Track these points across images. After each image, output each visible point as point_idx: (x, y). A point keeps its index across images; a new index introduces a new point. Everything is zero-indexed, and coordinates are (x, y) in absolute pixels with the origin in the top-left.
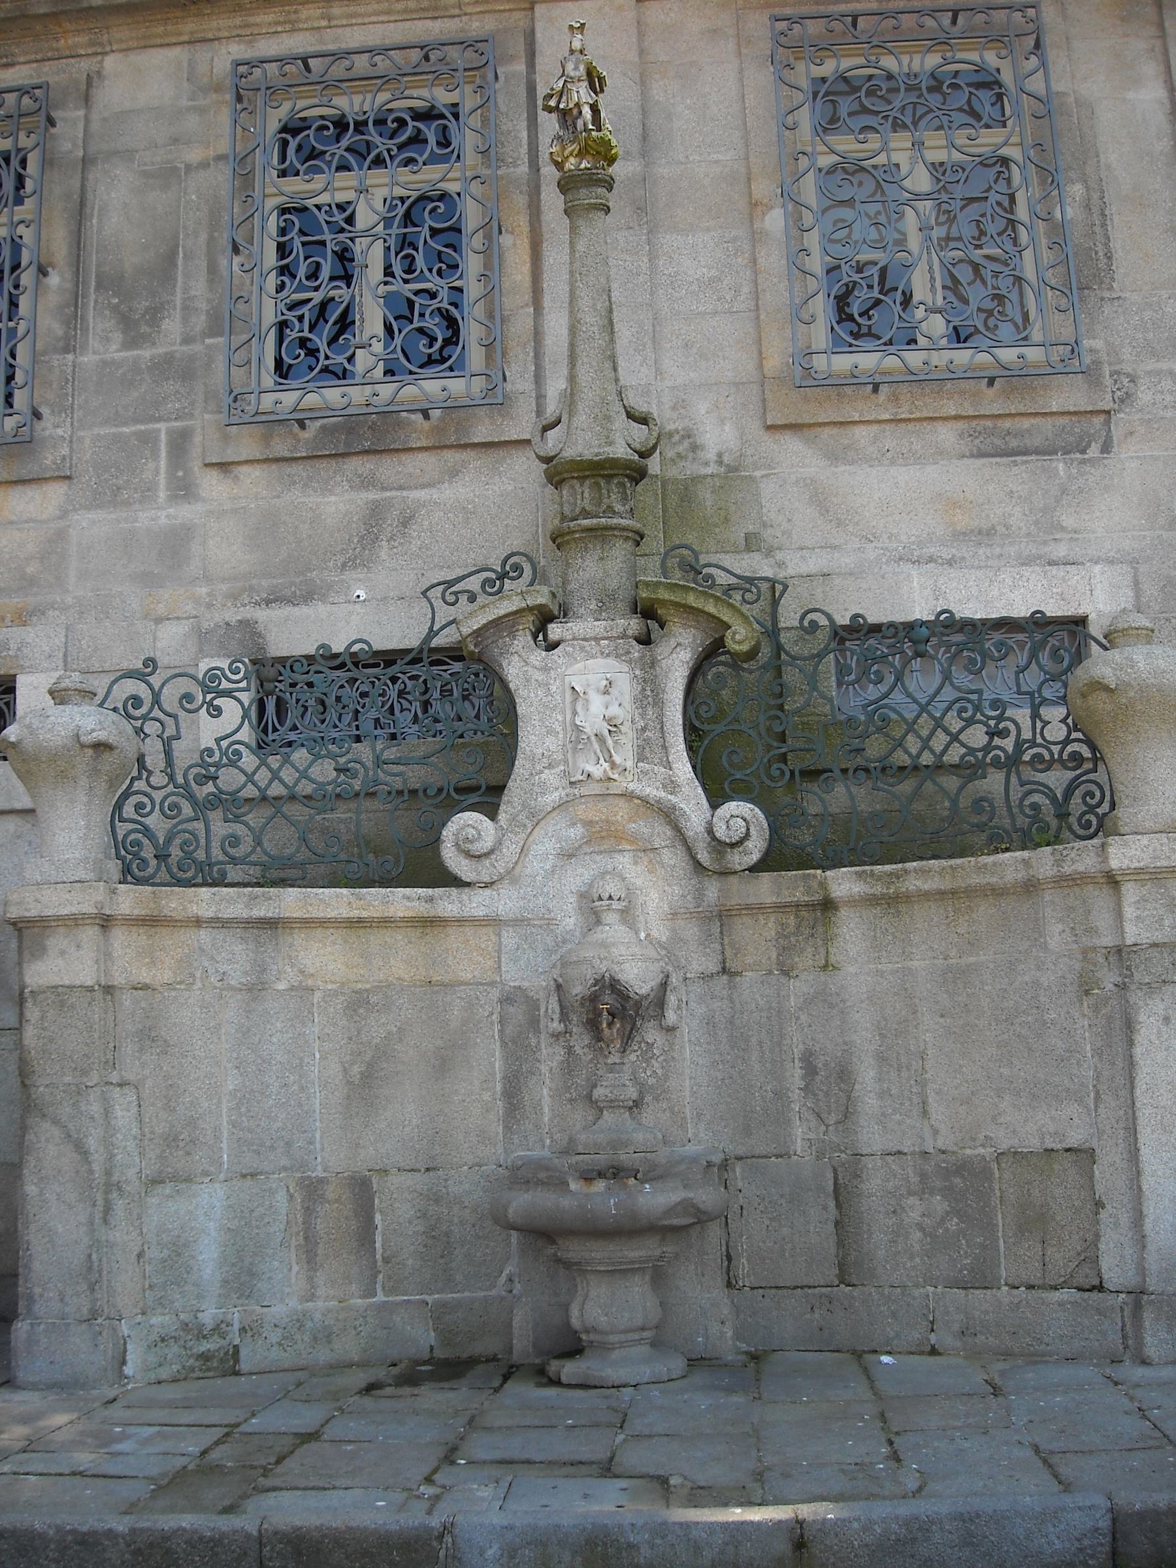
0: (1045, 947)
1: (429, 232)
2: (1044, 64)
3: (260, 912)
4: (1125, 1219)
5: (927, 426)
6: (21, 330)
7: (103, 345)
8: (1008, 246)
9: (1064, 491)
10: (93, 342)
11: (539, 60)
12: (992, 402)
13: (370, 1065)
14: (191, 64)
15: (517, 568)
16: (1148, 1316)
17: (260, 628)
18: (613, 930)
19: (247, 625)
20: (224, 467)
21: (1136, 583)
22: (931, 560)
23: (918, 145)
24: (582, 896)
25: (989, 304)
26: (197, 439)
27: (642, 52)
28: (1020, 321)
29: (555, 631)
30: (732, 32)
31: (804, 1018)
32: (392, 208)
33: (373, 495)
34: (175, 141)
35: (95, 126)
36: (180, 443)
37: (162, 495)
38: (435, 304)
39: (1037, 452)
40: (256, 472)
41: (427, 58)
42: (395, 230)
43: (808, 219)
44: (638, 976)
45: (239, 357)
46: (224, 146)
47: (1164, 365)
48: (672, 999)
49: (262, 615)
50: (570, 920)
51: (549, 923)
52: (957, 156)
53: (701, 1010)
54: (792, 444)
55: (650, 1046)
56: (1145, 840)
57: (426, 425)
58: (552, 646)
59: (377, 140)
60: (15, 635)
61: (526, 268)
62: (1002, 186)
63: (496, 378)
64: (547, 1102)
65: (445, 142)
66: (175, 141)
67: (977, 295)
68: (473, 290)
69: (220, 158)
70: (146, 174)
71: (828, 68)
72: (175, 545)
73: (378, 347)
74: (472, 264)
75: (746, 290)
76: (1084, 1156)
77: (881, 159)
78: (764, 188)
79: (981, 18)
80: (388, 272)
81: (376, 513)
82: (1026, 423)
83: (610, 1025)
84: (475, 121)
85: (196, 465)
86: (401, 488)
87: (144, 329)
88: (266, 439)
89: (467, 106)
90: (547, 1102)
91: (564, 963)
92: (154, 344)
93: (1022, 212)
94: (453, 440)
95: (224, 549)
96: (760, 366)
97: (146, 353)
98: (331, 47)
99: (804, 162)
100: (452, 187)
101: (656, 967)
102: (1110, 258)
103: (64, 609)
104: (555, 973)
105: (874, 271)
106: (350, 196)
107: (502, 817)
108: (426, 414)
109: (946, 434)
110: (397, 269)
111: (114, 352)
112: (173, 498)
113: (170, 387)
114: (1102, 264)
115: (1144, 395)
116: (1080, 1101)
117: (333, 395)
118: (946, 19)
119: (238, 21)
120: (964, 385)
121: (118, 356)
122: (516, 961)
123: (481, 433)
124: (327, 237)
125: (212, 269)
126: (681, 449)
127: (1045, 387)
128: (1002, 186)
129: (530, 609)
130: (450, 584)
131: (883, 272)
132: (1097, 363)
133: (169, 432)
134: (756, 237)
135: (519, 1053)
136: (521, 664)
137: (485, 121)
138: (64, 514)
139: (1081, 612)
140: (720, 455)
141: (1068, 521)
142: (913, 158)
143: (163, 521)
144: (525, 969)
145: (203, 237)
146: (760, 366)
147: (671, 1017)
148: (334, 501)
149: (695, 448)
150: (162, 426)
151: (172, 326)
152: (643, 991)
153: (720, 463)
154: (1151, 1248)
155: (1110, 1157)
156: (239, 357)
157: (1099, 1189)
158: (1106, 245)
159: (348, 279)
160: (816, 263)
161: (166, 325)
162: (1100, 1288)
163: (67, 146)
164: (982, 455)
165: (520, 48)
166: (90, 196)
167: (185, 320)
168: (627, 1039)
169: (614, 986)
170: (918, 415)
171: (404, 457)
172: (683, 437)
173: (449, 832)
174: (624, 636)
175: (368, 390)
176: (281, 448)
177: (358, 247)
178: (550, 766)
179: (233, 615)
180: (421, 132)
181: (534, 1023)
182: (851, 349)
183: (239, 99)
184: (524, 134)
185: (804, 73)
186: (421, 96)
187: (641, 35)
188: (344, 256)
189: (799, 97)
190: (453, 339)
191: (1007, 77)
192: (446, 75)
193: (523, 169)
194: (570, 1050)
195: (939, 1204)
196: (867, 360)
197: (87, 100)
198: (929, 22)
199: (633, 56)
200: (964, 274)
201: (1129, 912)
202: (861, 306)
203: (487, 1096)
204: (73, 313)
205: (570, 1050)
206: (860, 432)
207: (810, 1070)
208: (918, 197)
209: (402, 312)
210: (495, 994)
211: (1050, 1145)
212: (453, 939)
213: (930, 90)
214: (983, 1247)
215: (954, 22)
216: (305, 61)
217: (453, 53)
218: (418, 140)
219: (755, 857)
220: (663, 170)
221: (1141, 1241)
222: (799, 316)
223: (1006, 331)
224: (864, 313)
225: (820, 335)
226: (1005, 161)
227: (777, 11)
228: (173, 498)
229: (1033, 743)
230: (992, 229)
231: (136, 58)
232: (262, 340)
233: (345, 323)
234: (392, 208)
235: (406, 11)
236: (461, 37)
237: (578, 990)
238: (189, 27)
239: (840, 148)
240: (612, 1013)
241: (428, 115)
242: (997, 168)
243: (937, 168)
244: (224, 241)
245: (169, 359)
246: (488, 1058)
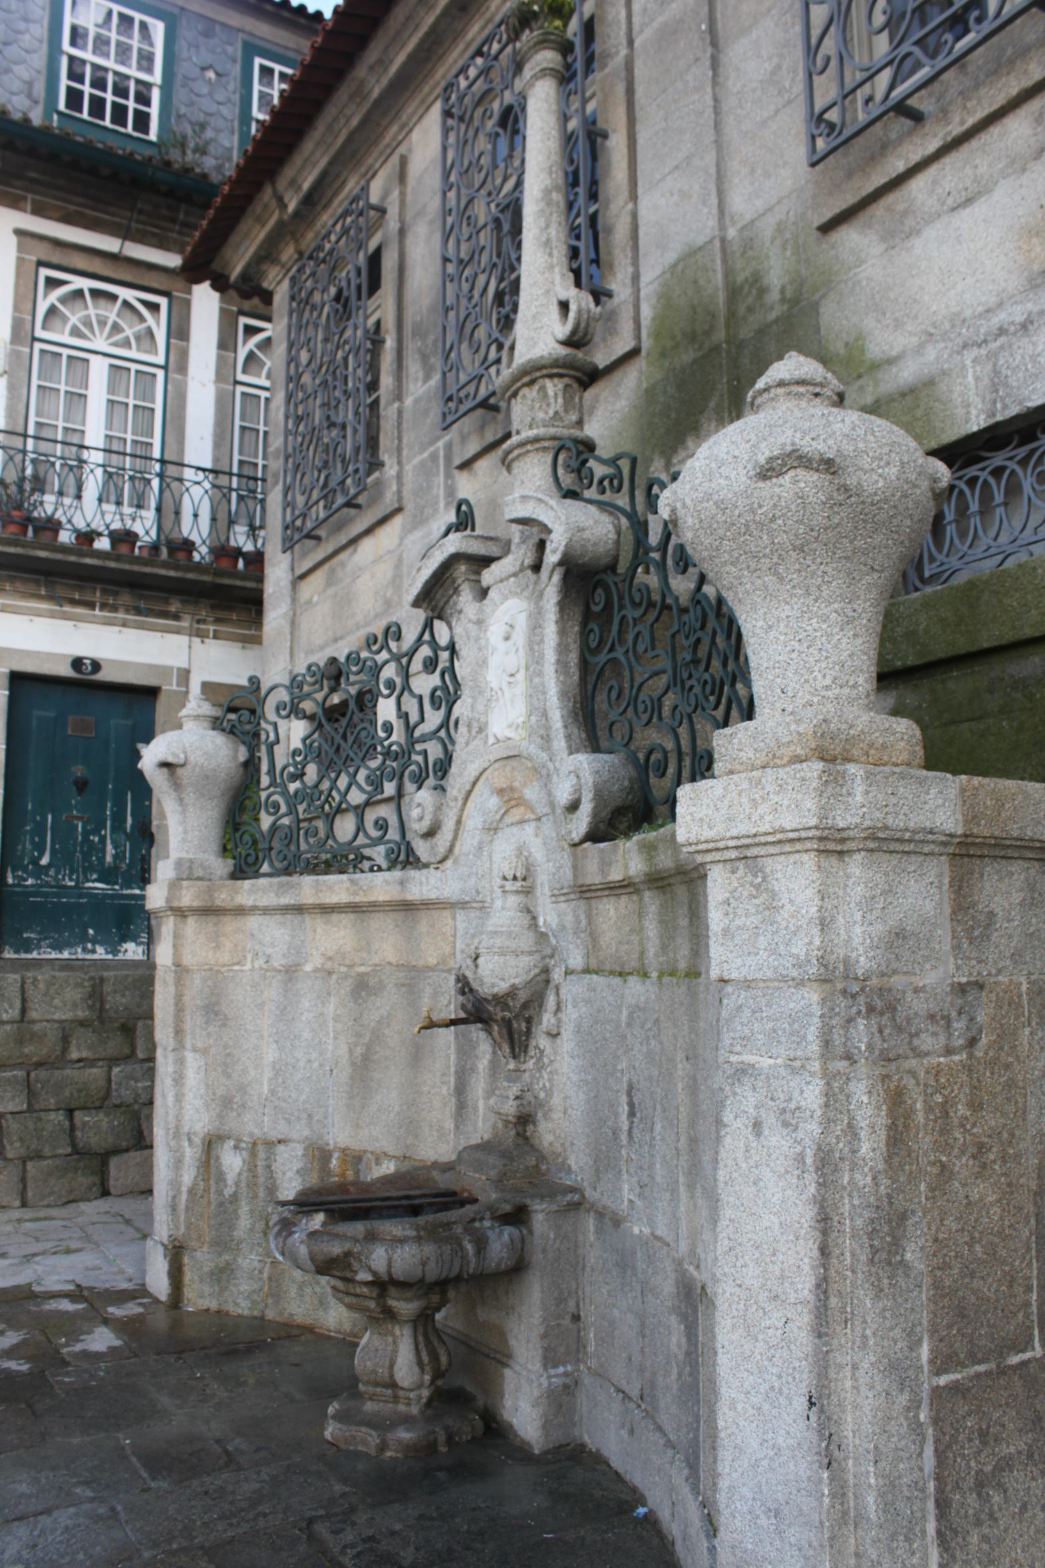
20: (466, 465)
54: (850, 237)
119: (461, 46)
126: (750, 300)
153: (783, 300)
170: (970, 122)
172: (751, 285)
206: (918, 185)
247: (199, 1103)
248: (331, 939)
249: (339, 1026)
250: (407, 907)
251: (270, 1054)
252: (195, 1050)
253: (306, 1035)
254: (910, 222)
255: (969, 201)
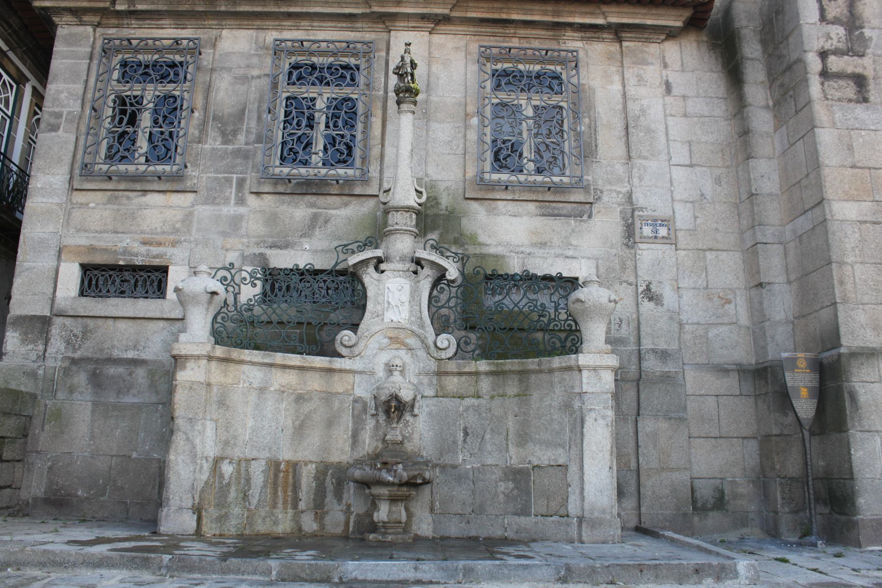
0: (554, 393)
1: (345, 113)
2: (578, 73)
3: (267, 361)
4: (577, 491)
5: (525, 203)
6: (181, 133)
7: (213, 142)
8: (560, 139)
9: (573, 231)
10: (210, 141)
11: (391, 52)
12: (549, 197)
13: (302, 421)
14: (257, 37)
15: (370, 242)
16: (584, 525)
17: (267, 257)
18: (397, 377)
19: (261, 254)
21: (597, 267)
22: (522, 252)
23: (529, 99)
24: (386, 364)
25: (551, 160)
26: (248, 182)
27: (430, 53)
28: (561, 166)
29: (383, 266)
30: (464, 49)
31: (465, 415)
32: (331, 102)
33: (314, 210)
34: (248, 66)
35: (217, 57)
36: (241, 183)
37: (233, 202)
38: (344, 140)
39: (564, 216)
40: (270, 197)
41: (348, 47)
42: (332, 111)
43: (487, 122)
44: (406, 395)
45: (267, 153)
46: (267, 71)
47: (613, 188)
48: (417, 405)
49: (268, 252)
50: (381, 374)
51: (372, 373)
52: (543, 104)
53: (427, 410)
55: (408, 422)
56: (591, 355)
57: (337, 186)
58: (383, 272)
59: (328, 75)
60: (169, 251)
61: (380, 130)
62: (559, 117)
63: (364, 172)
64: (367, 441)
65: (353, 80)
66: (248, 66)
67: (547, 156)
68: (359, 136)
69: (265, 75)
70: (235, 77)
71: (499, 66)
72: (236, 222)
73: (321, 154)
74: (360, 127)
75: (461, 146)
76: (564, 467)
77: (516, 102)
78: (471, 109)
79: (556, 54)
80: (327, 126)
81: (315, 218)
82: (561, 205)
83: (394, 412)
84: (365, 73)
85: (247, 192)
86: (325, 208)
87: (230, 137)
88: (276, 184)
89: (362, 67)
90: (367, 441)
91: (378, 388)
92: (234, 144)
93: (566, 127)
94: (347, 192)
95: (254, 226)
96: (464, 176)
97: (230, 147)
98: (312, 38)
99: (487, 101)
100: (354, 96)
101: (412, 392)
102: (596, 147)
103: (190, 242)
104: (375, 392)
105: (510, 144)
106: (315, 95)
107: (359, 333)
108: (337, 181)
109: (531, 207)
110: (331, 125)
111: (218, 145)
112: (237, 204)
113: (239, 161)
114: (594, 148)
115: (605, 198)
116: (564, 448)
117: (303, 171)
118: (544, 53)
119: (277, 23)
120: (540, 189)
121: (220, 147)
122: (359, 386)
123: (358, 191)
124: (306, 111)
125: (259, 118)
127: (569, 192)
128: (559, 117)
129: (374, 258)
130: (345, 246)
131: (513, 145)
132: (589, 185)
133: (237, 178)
134: (466, 127)
135: (358, 421)
136: (369, 277)
137: (369, 73)
138: (193, 206)
139: (576, 276)
140: (447, 207)
141: (574, 242)
142: (527, 104)
143: (232, 212)
144: (362, 390)
145: (256, 105)
146: (464, 176)
147: (416, 411)
148: (298, 211)
149: (438, 204)
150: (235, 176)
151: (241, 138)
152: (407, 400)
153: (447, 210)
154: (586, 501)
155: (573, 468)
156: (267, 153)
157: (569, 480)
158: (596, 141)
159: (312, 127)
160: (488, 139)
161: (239, 137)
162: (568, 516)
163: (205, 63)
164: (544, 215)
165: (383, 46)
166: (213, 84)
167: (246, 137)
168: (399, 418)
169: (396, 397)
171: (328, 197)
173: (338, 337)
174: (408, 270)
175: (316, 171)
176: (280, 189)
177: (317, 115)
178: (378, 316)
179: (257, 251)
180: (345, 74)
181: (365, 410)
182: (498, 172)
183: (275, 54)
184: (383, 80)
185: (489, 67)
186: (345, 60)
187: (430, 47)
188: (311, 118)
189: (487, 77)
190: (350, 154)
191: (564, 77)
192: (355, 55)
193: (382, 93)
194: (378, 421)
195: (511, 485)
196: (504, 177)
197: (214, 46)
198: (537, 53)
199: (426, 54)
200: (542, 148)
201: (584, 380)
202: (504, 155)
203: (345, 436)
204: (203, 127)
205: (378, 421)
206: (499, 203)
207: (466, 434)
208: (528, 118)
209: (332, 141)
210: (351, 398)
211: (552, 463)
212: (336, 377)
213: (536, 78)
214: (526, 501)
215: (546, 54)
216: (302, 42)
217: (359, 46)
218: (343, 77)
219: (451, 355)
220: (433, 98)
221: (583, 499)
222: (481, 159)
223: (556, 170)
224: (505, 159)
225: (488, 166)
226: (561, 108)
227: (482, 44)
228: (237, 204)
229: (554, 320)
230: (554, 132)
231: (235, 32)
232: (277, 147)
233: (309, 144)
234: (331, 102)
235: (342, 27)
236: (362, 40)
237: (383, 398)
238: (258, 23)
239: (500, 97)
240: (395, 408)
241: (346, 67)
242: (557, 110)
243: (536, 108)
244: (265, 107)
245: (239, 150)
246: (347, 421)
247: (212, 443)
248: (290, 378)
249: (288, 413)
250: (330, 371)
251: (250, 423)
252: (211, 420)
253: (270, 415)
254: (495, 212)
255: (515, 216)
